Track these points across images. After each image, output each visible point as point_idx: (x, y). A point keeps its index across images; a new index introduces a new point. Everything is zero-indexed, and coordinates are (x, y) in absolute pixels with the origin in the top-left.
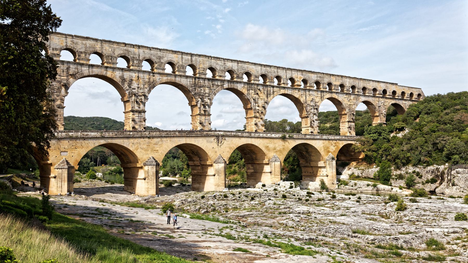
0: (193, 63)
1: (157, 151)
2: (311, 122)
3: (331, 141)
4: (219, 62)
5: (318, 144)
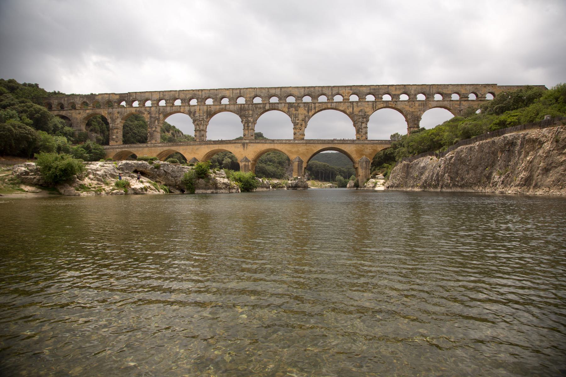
4: (263, 91)
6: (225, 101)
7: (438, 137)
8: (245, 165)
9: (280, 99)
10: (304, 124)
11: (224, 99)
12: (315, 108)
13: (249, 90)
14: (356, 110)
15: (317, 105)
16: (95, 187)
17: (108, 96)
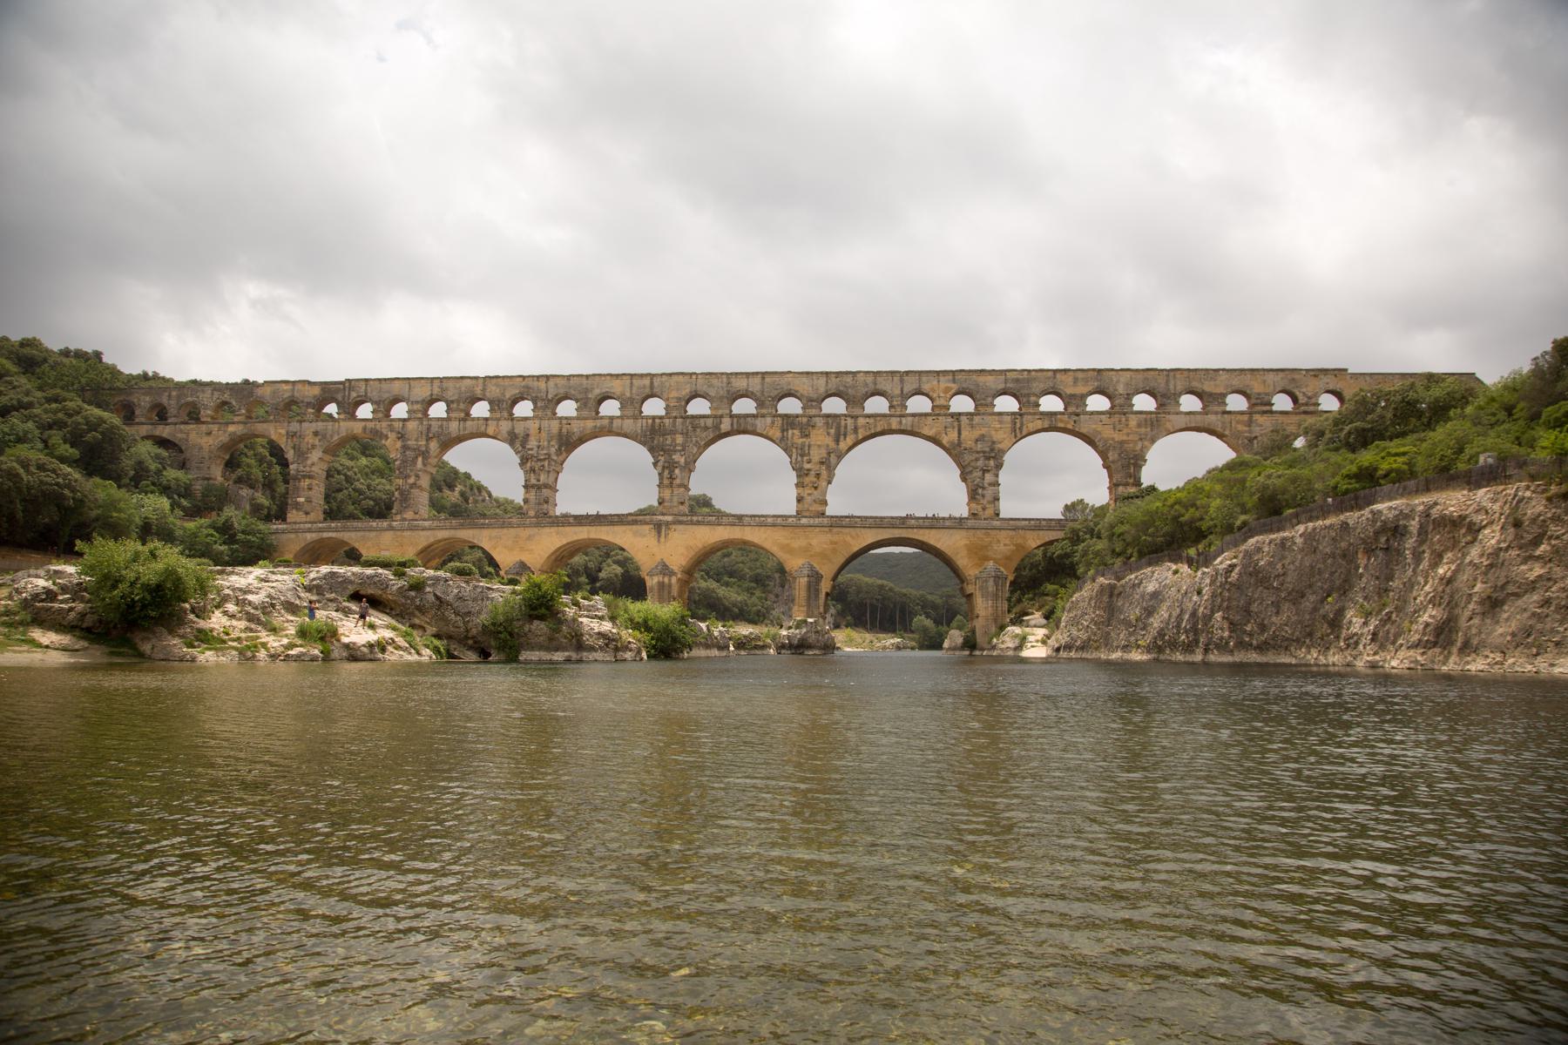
3: (993, 533)
4: (715, 381)
6: (610, 408)
7: (1192, 510)
8: (661, 585)
9: (760, 404)
10: (824, 473)
11: (698, 400)
12: (856, 430)
13: (675, 378)
14: (968, 436)
15: (861, 421)
16: (238, 639)
17: (289, 387)
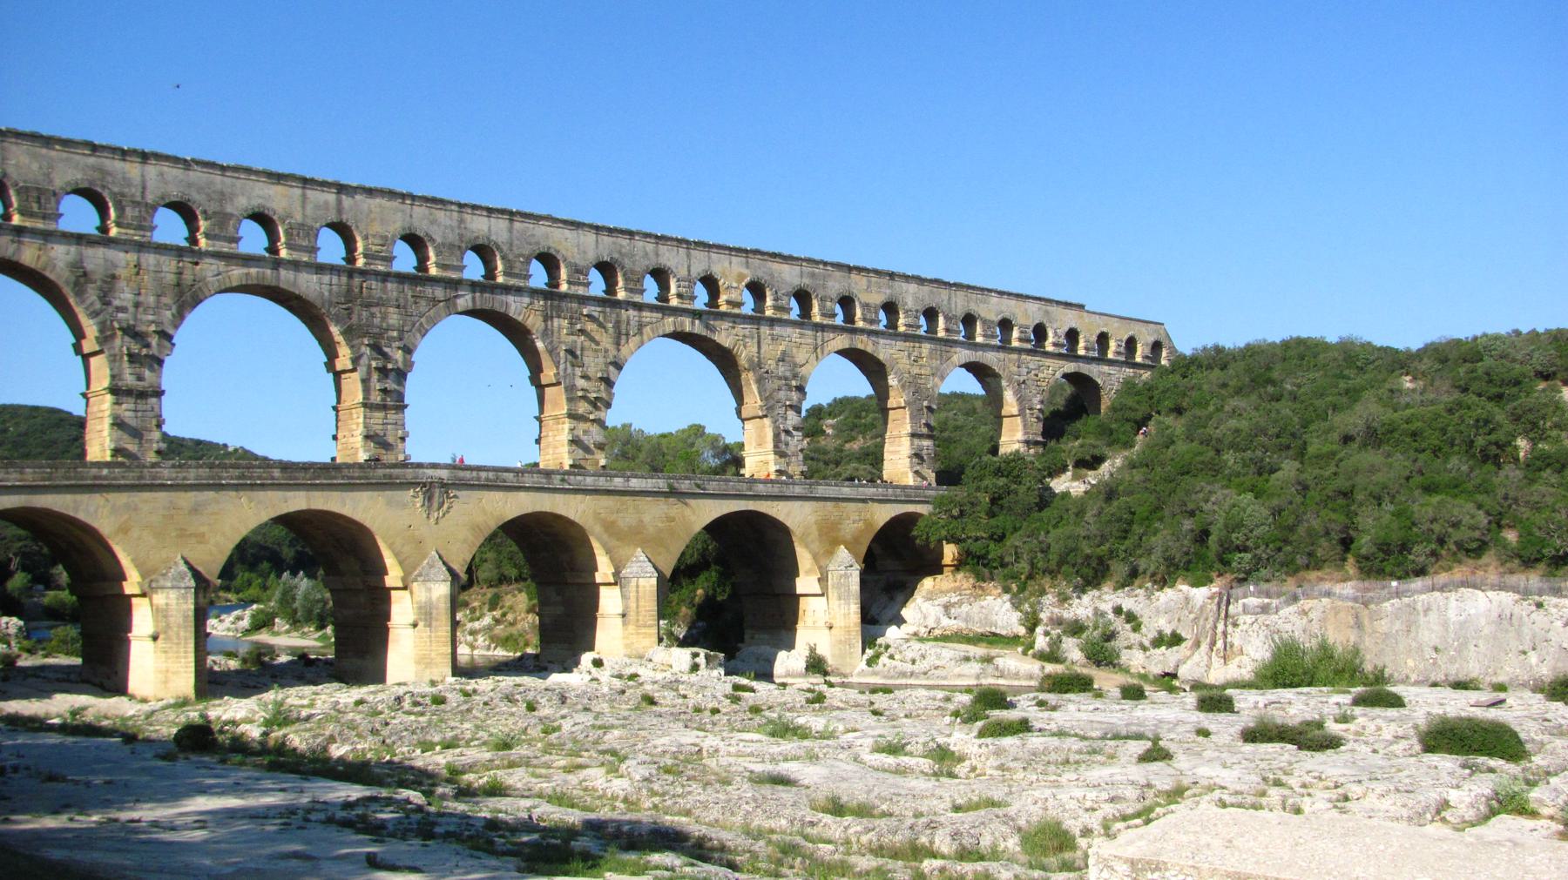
0: (344, 217)
1: (203, 535)
2: (777, 437)
4: (441, 215)
5: (794, 515)
14: (771, 351)
